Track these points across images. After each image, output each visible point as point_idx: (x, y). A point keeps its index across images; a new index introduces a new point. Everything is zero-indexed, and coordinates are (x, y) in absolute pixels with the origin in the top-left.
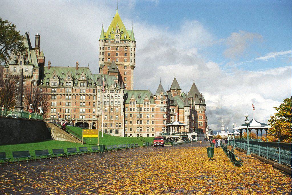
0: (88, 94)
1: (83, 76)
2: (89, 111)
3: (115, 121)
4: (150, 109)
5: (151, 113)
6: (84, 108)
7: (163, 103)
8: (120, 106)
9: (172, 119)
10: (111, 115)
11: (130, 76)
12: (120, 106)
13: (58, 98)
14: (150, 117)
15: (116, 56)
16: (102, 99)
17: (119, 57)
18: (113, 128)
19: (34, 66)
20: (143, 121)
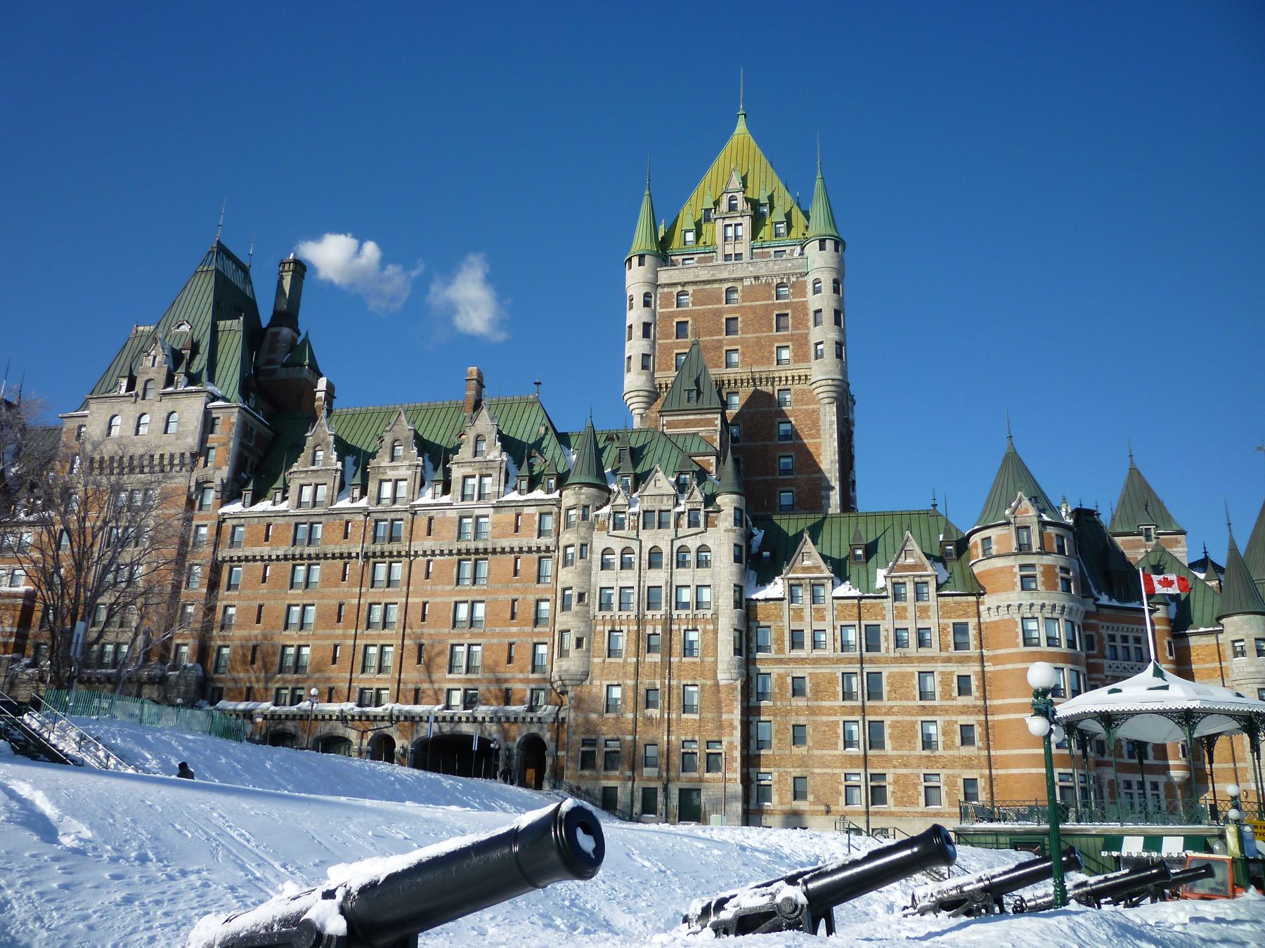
0: (506, 543)
4: (942, 630)
5: (948, 660)
7: (1040, 579)
8: (709, 613)
10: (645, 682)
13: (326, 580)
14: (947, 695)
15: (723, 336)
16: (587, 571)
17: (742, 342)
18: (660, 777)
20: (894, 725)
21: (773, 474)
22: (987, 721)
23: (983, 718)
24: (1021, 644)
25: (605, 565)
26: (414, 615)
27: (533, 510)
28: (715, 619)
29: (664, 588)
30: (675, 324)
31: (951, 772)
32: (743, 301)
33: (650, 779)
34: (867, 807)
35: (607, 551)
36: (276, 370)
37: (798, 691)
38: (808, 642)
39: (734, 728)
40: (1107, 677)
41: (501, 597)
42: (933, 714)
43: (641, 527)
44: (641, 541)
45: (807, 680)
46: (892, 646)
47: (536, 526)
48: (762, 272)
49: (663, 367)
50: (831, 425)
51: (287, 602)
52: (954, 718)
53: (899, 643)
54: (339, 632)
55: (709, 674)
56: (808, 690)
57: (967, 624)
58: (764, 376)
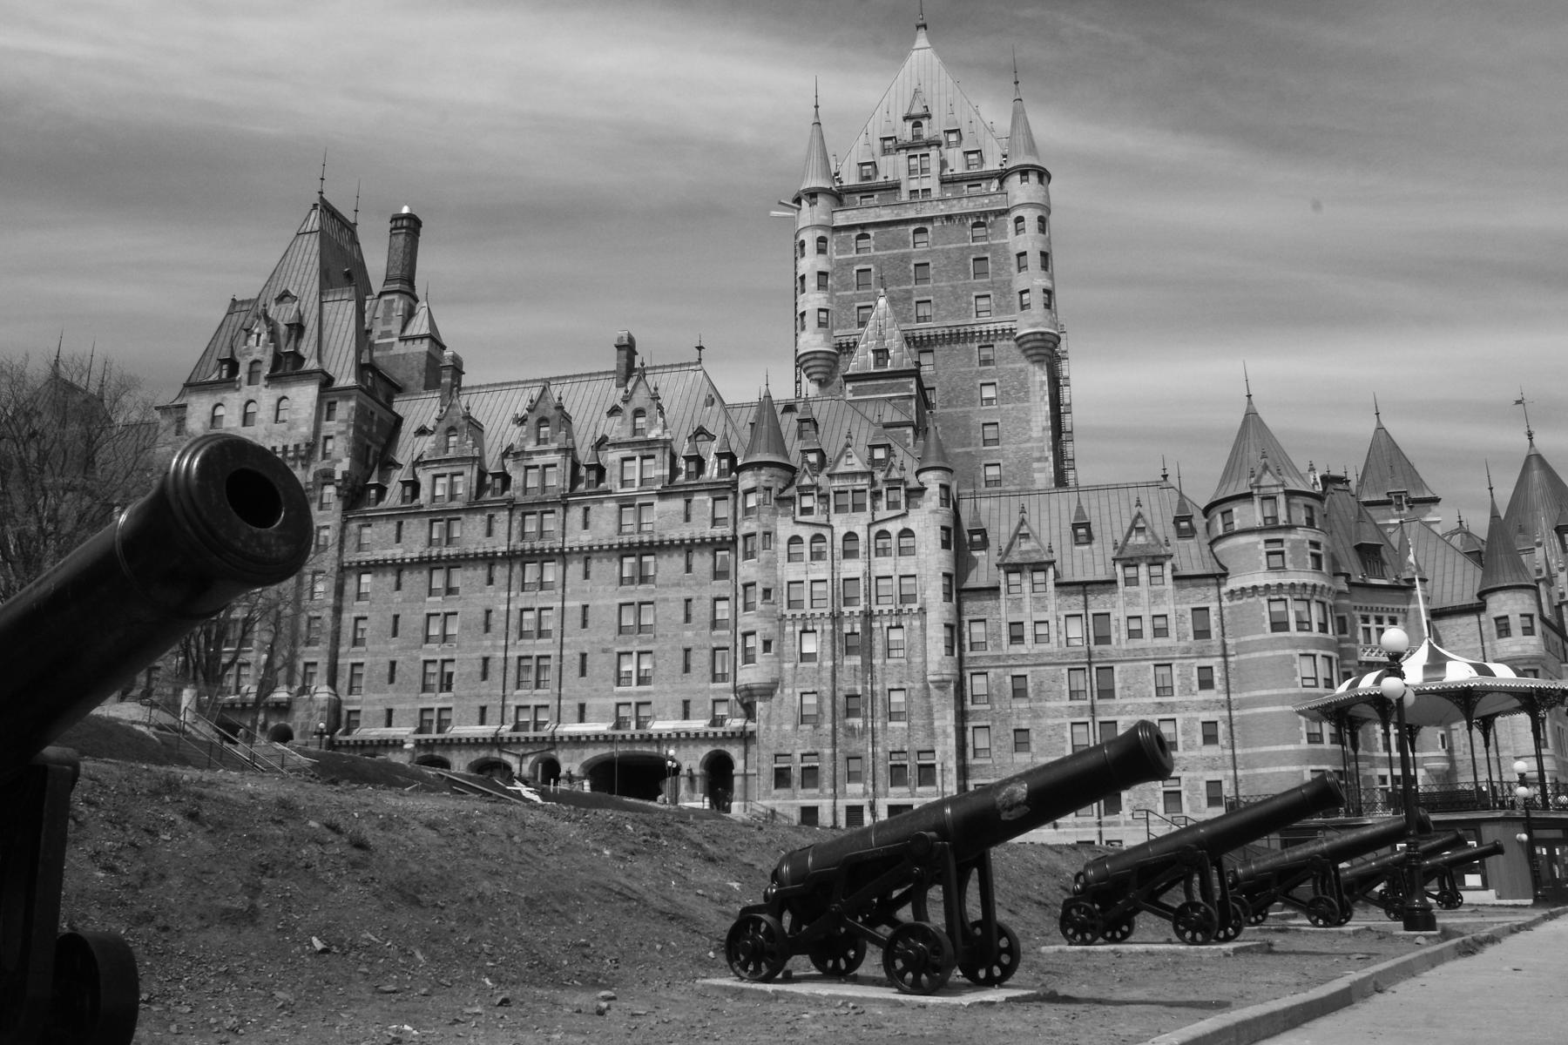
0: (674, 534)
1: (639, 412)
2: (687, 669)
3: (879, 738)
6: (649, 641)
7: (1288, 556)
8: (915, 607)
11: (1027, 411)
12: (915, 607)
16: (771, 564)
18: (865, 794)
19: (326, 382)
21: (976, 445)
22: (1230, 717)
23: (1226, 713)
24: (1268, 629)
26: (573, 620)
28: (923, 611)
29: (861, 580)
33: (855, 796)
34: (1099, 817)
35: (795, 540)
36: (393, 343)
37: (1019, 692)
38: (1028, 635)
40: (1360, 662)
42: (1172, 712)
43: (832, 510)
44: (831, 527)
45: (1029, 679)
46: (1124, 636)
48: (955, 211)
49: (843, 323)
50: (1041, 386)
51: (426, 611)
52: (1195, 715)
53: (1134, 634)
54: (488, 643)
55: (919, 677)
56: (1030, 690)
57: (1207, 609)
58: (962, 331)
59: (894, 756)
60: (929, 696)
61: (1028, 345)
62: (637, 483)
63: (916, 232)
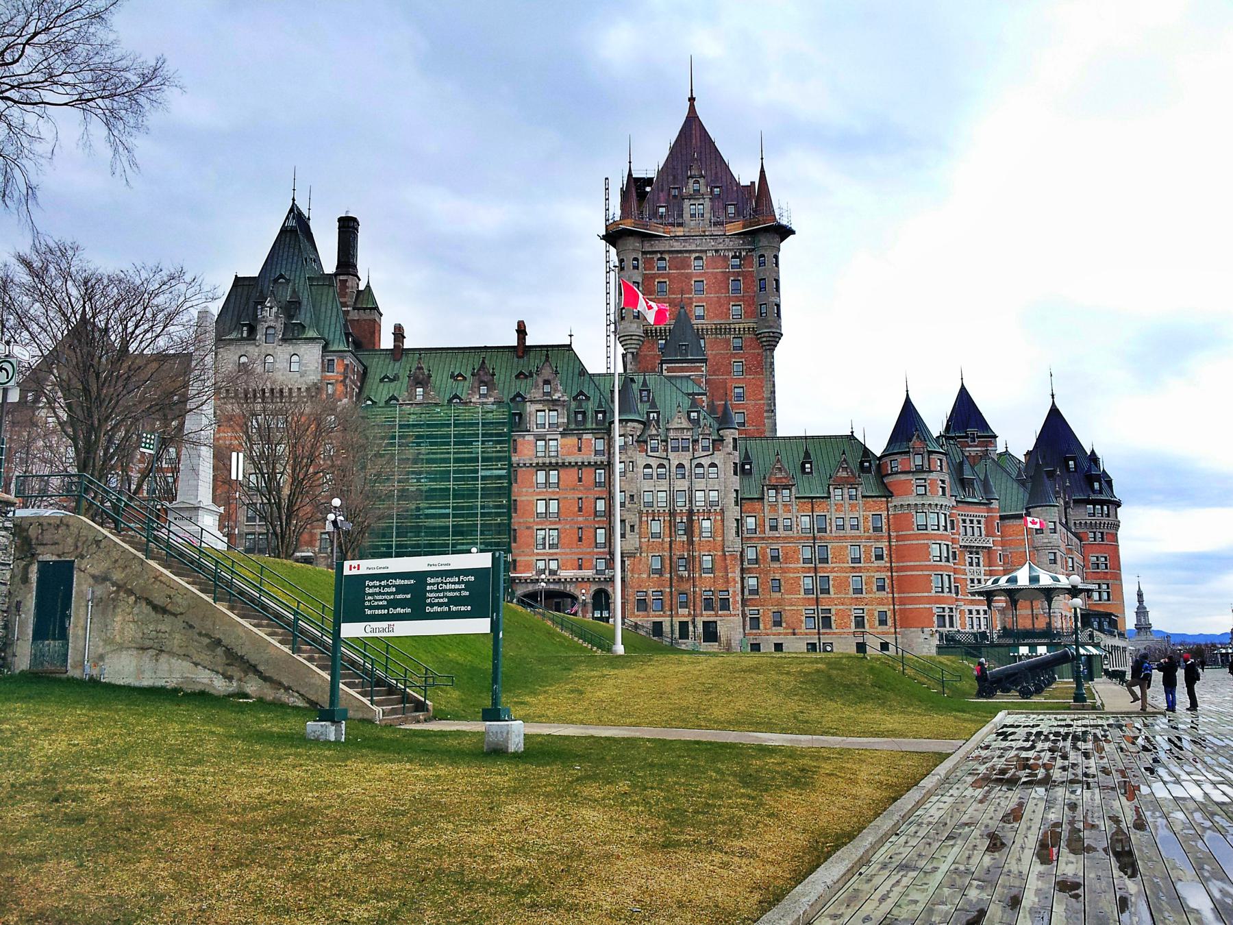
0: (572, 459)
2: (580, 539)
6: (555, 523)
7: (928, 488)
8: (718, 509)
9: (974, 568)
14: (869, 560)
18: (689, 614)
22: (892, 576)
25: (646, 477)
27: (590, 436)
30: (656, 283)
31: (870, 607)
32: (708, 268)
33: (683, 616)
34: (819, 630)
37: (775, 559)
39: (737, 583)
41: (570, 496)
44: (669, 460)
46: (834, 529)
47: (593, 448)
48: (721, 246)
59: (705, 593)
60: (726, 559)
61: (765, 339)
62: (547, 426)
63: (696, 258)
